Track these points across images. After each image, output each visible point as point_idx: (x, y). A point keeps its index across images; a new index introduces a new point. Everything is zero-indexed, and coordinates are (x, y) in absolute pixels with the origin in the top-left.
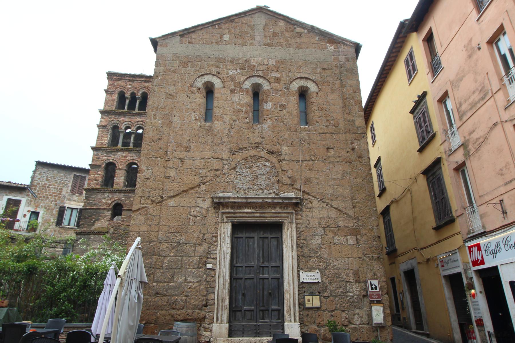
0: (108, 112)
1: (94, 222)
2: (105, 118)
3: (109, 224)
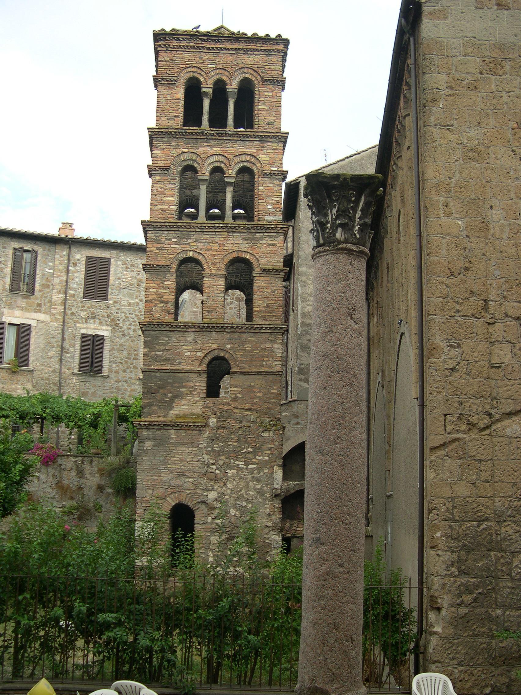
0: (171, 132)
1: (172, 400)
2: (163, 149)
3: (207, 406)
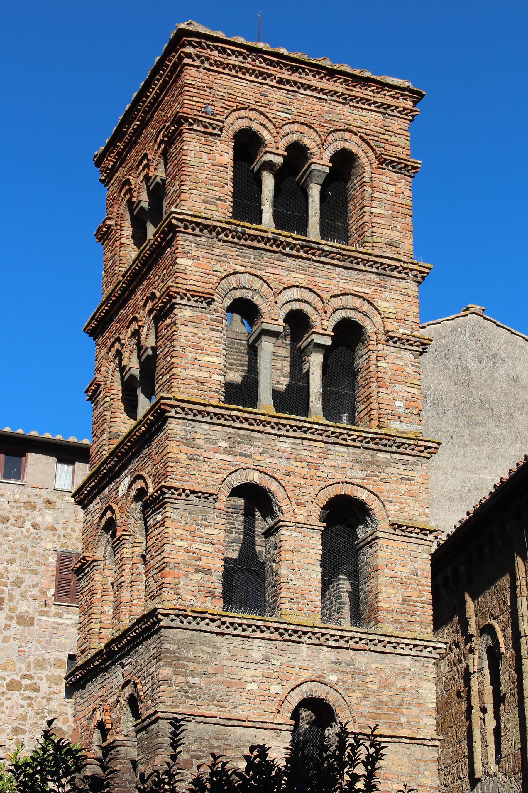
2: (198, 258)
